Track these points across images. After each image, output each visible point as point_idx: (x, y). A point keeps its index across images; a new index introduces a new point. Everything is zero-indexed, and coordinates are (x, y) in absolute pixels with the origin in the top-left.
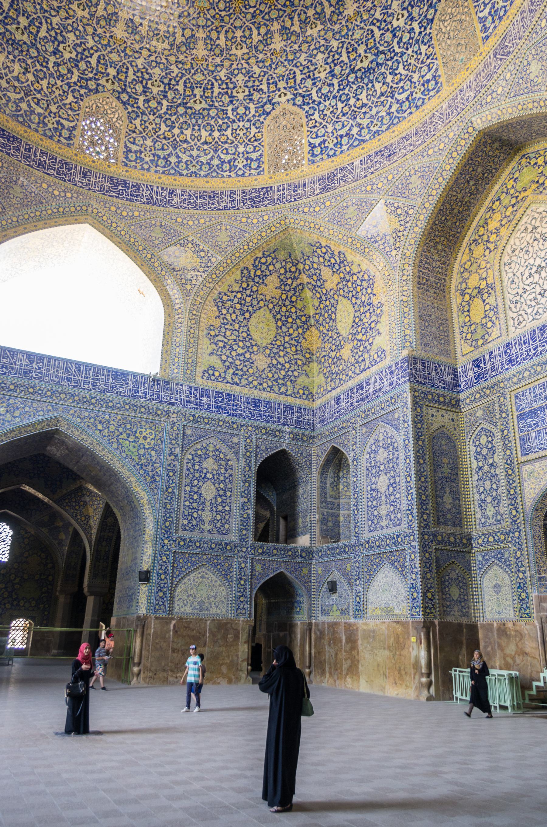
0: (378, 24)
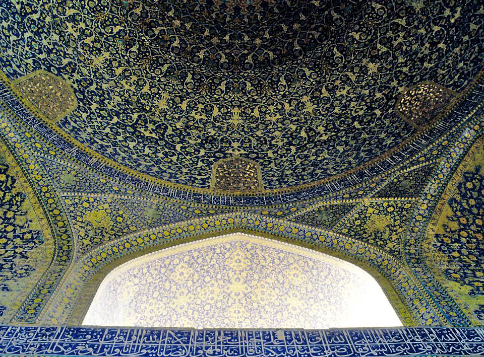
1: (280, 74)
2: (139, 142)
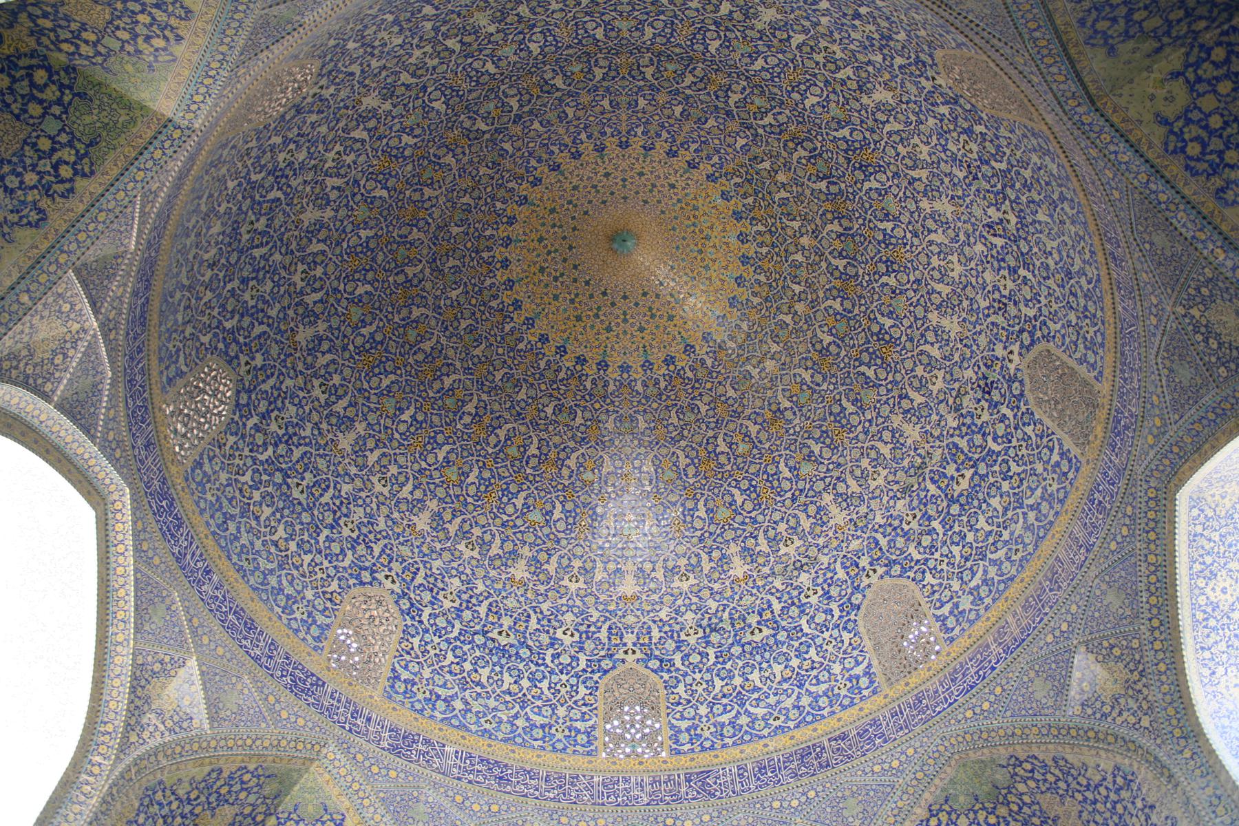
0: (540, 616)
1: (872, 225)
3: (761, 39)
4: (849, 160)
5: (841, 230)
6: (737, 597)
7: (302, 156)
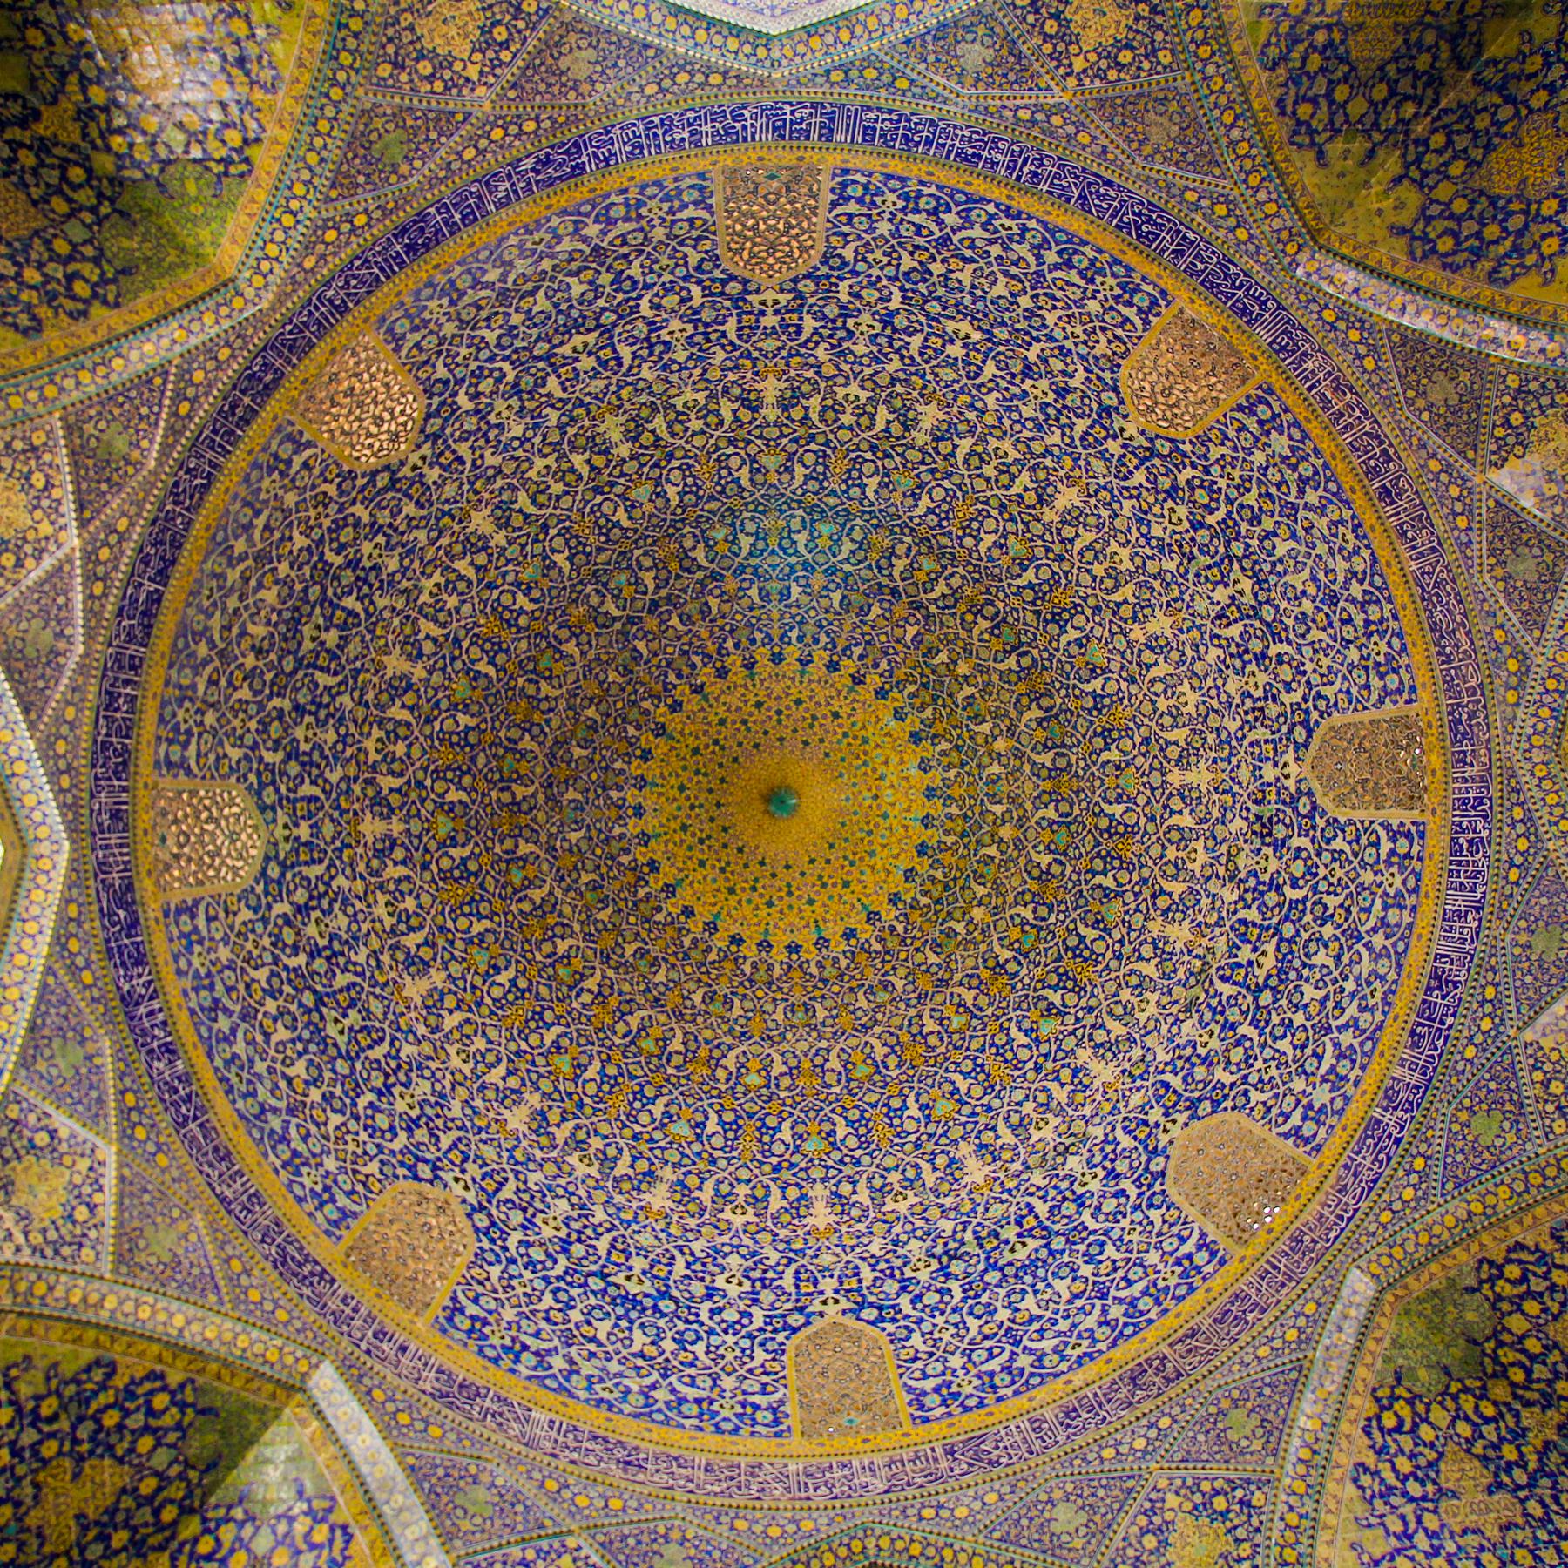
2: (1300, 977)
3: (923, 462)
4: (1037, 613)
5: (1041, 714)
6: (980, 1209)
7: (392, 564)
